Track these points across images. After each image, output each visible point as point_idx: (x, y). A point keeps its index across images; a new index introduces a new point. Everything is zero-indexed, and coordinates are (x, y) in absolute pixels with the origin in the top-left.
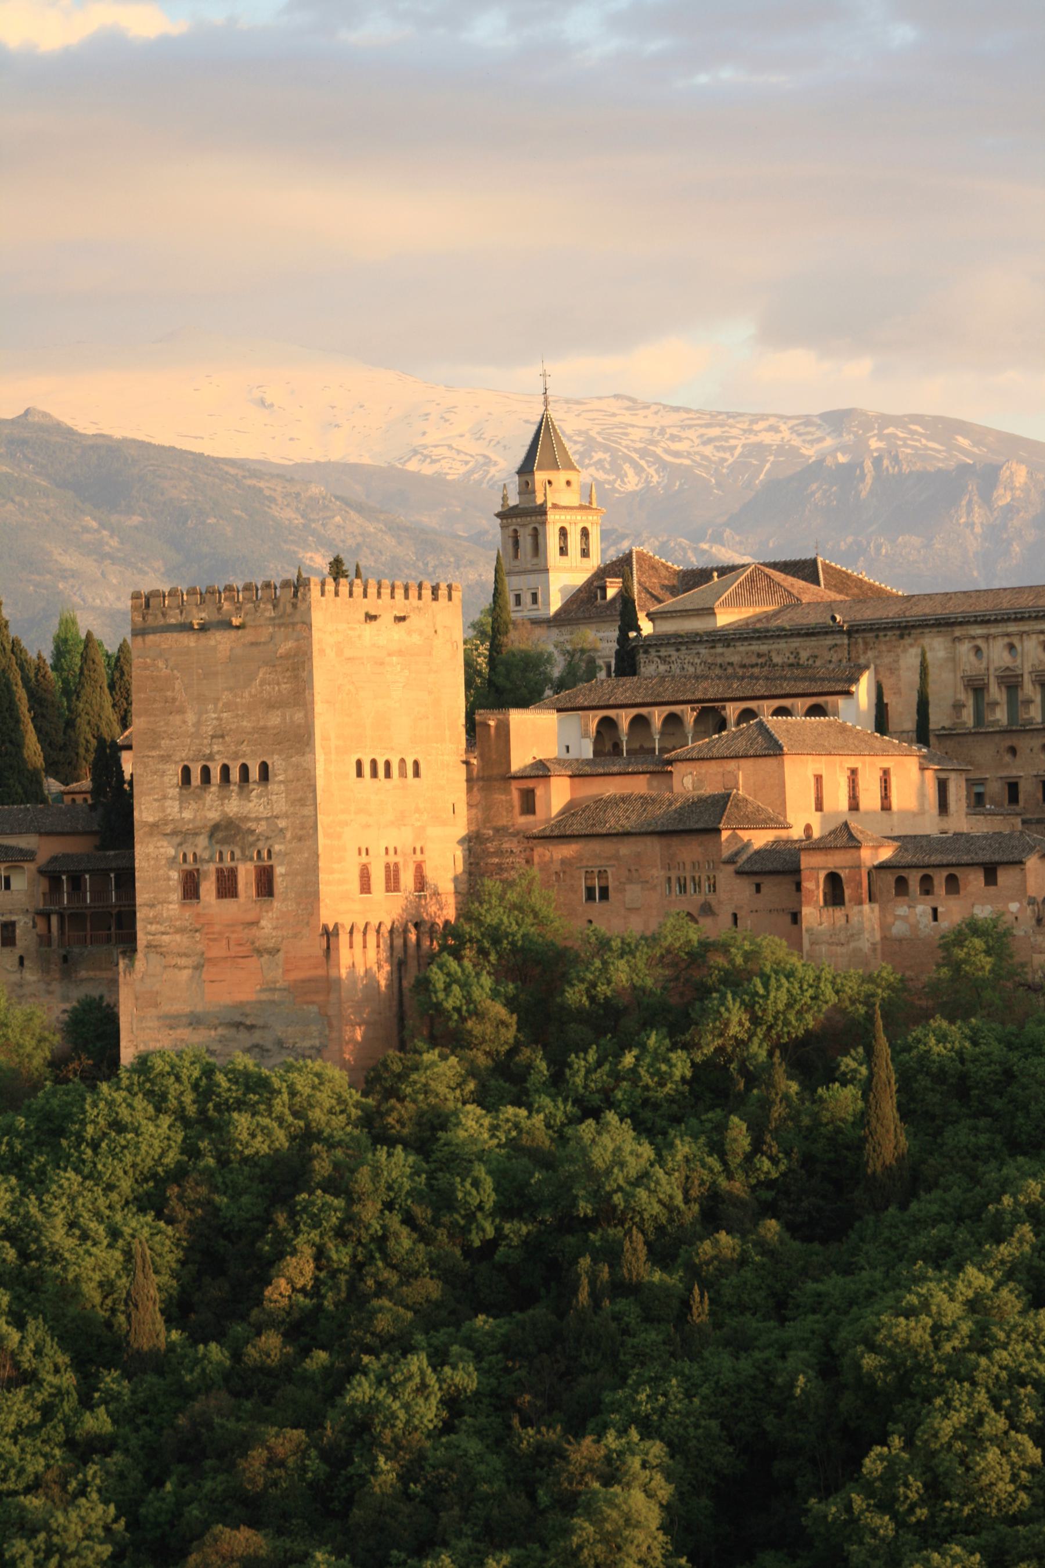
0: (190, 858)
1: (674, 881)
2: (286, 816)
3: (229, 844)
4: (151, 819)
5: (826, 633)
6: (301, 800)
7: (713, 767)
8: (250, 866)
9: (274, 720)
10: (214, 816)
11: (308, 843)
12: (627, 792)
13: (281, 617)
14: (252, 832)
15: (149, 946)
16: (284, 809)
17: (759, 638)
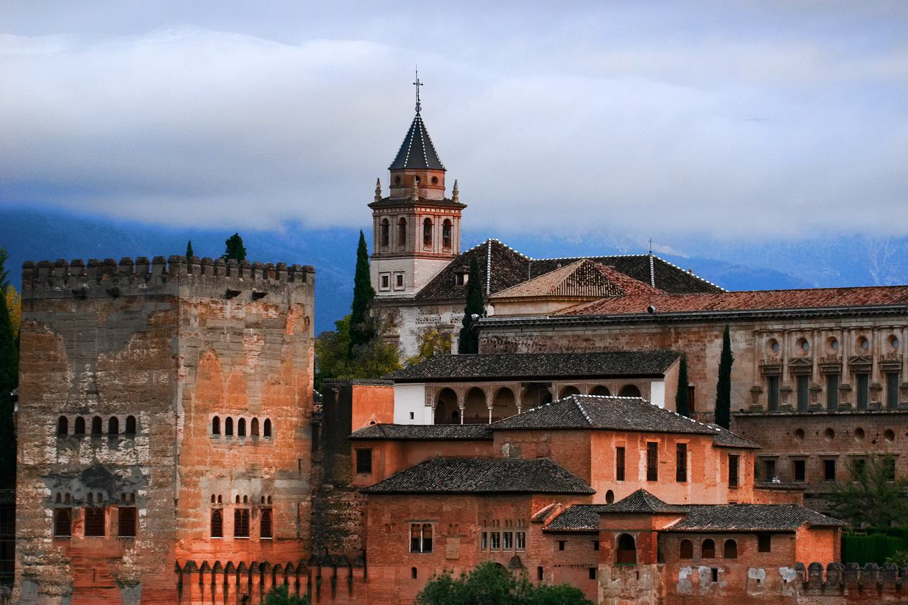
0: (63, 498)
1: (489, 535)
2: (149, 465)
4: (31, 463)
5: (642, 323)
6: (163, 451)
7: (529, 438)
9: (142, 379)
10: (85, 461)
12: (453, 454)
14: (119, 477)
17: (584, 325)
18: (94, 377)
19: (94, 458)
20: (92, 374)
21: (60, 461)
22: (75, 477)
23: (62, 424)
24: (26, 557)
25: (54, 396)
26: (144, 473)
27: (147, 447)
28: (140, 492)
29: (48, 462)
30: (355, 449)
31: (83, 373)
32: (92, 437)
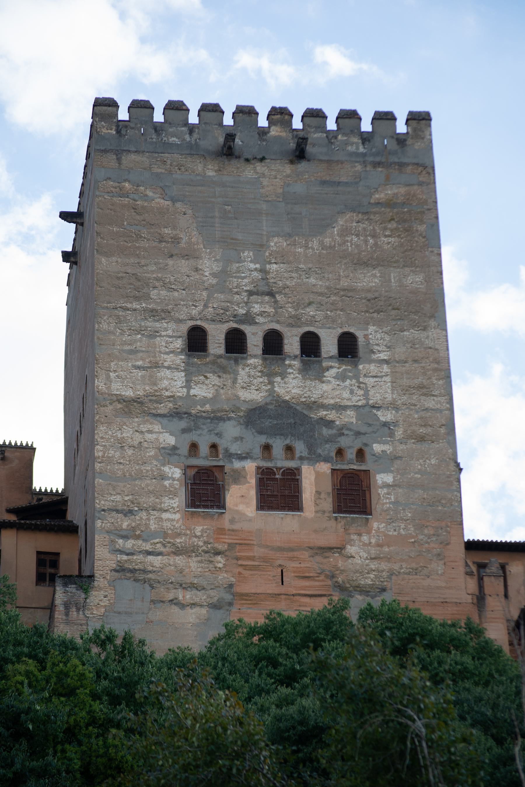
0: (204, 449)
2: (394, 406)
3: (285, 436)
4: (129, 393)
6: (421, 387)
8: (325, 468)
11: (435, 445)
13: (378, 154)
15: (120, 569)
16: (389, 397)
18: (263, 271)
19: (271, 392)
20: (258, 266)
21: (192, 392)
22: (229, 419)
24: (121, 541)
25: (176, 294)
26: (383, 419)
27: (388, 379)
28: (377, 448)
29: (167, 394)
30: (474, 563)
31: (237, 265)
32: (264, 360)
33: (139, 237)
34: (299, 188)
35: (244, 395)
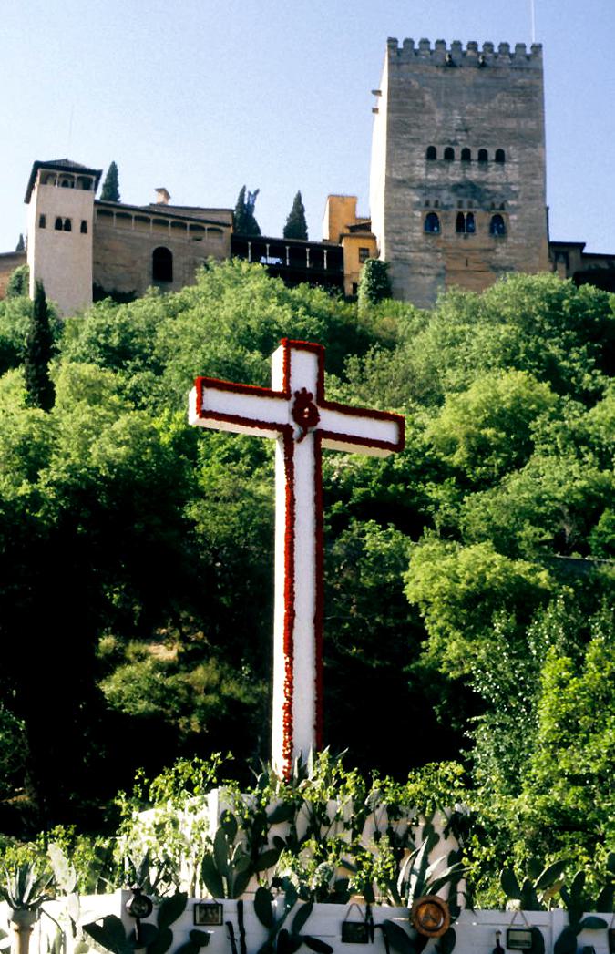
0: (432, 204)
2: (518, 183)
4: (400, 177)
9: (511, 124)
10: (457, 179)
14: (488, 191)
19: (464, 177)
23: (431, 154)
28: (510, 203)
33: (407, 104)
34: (480, 81)
35: (451, 178)
